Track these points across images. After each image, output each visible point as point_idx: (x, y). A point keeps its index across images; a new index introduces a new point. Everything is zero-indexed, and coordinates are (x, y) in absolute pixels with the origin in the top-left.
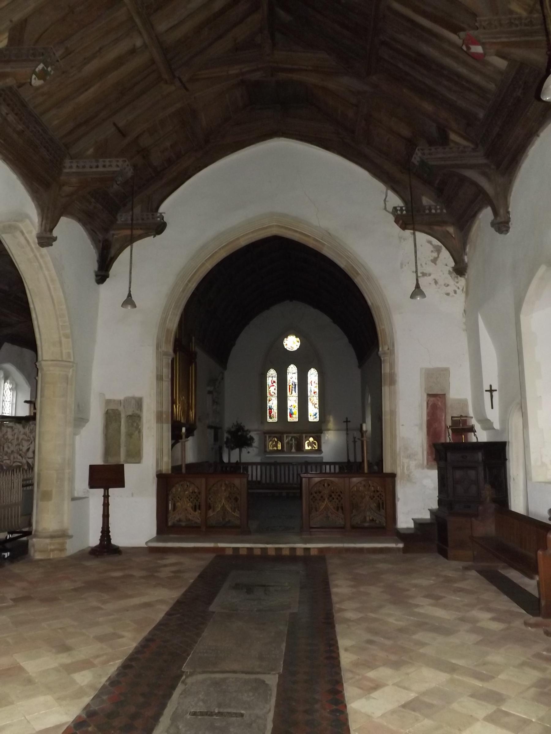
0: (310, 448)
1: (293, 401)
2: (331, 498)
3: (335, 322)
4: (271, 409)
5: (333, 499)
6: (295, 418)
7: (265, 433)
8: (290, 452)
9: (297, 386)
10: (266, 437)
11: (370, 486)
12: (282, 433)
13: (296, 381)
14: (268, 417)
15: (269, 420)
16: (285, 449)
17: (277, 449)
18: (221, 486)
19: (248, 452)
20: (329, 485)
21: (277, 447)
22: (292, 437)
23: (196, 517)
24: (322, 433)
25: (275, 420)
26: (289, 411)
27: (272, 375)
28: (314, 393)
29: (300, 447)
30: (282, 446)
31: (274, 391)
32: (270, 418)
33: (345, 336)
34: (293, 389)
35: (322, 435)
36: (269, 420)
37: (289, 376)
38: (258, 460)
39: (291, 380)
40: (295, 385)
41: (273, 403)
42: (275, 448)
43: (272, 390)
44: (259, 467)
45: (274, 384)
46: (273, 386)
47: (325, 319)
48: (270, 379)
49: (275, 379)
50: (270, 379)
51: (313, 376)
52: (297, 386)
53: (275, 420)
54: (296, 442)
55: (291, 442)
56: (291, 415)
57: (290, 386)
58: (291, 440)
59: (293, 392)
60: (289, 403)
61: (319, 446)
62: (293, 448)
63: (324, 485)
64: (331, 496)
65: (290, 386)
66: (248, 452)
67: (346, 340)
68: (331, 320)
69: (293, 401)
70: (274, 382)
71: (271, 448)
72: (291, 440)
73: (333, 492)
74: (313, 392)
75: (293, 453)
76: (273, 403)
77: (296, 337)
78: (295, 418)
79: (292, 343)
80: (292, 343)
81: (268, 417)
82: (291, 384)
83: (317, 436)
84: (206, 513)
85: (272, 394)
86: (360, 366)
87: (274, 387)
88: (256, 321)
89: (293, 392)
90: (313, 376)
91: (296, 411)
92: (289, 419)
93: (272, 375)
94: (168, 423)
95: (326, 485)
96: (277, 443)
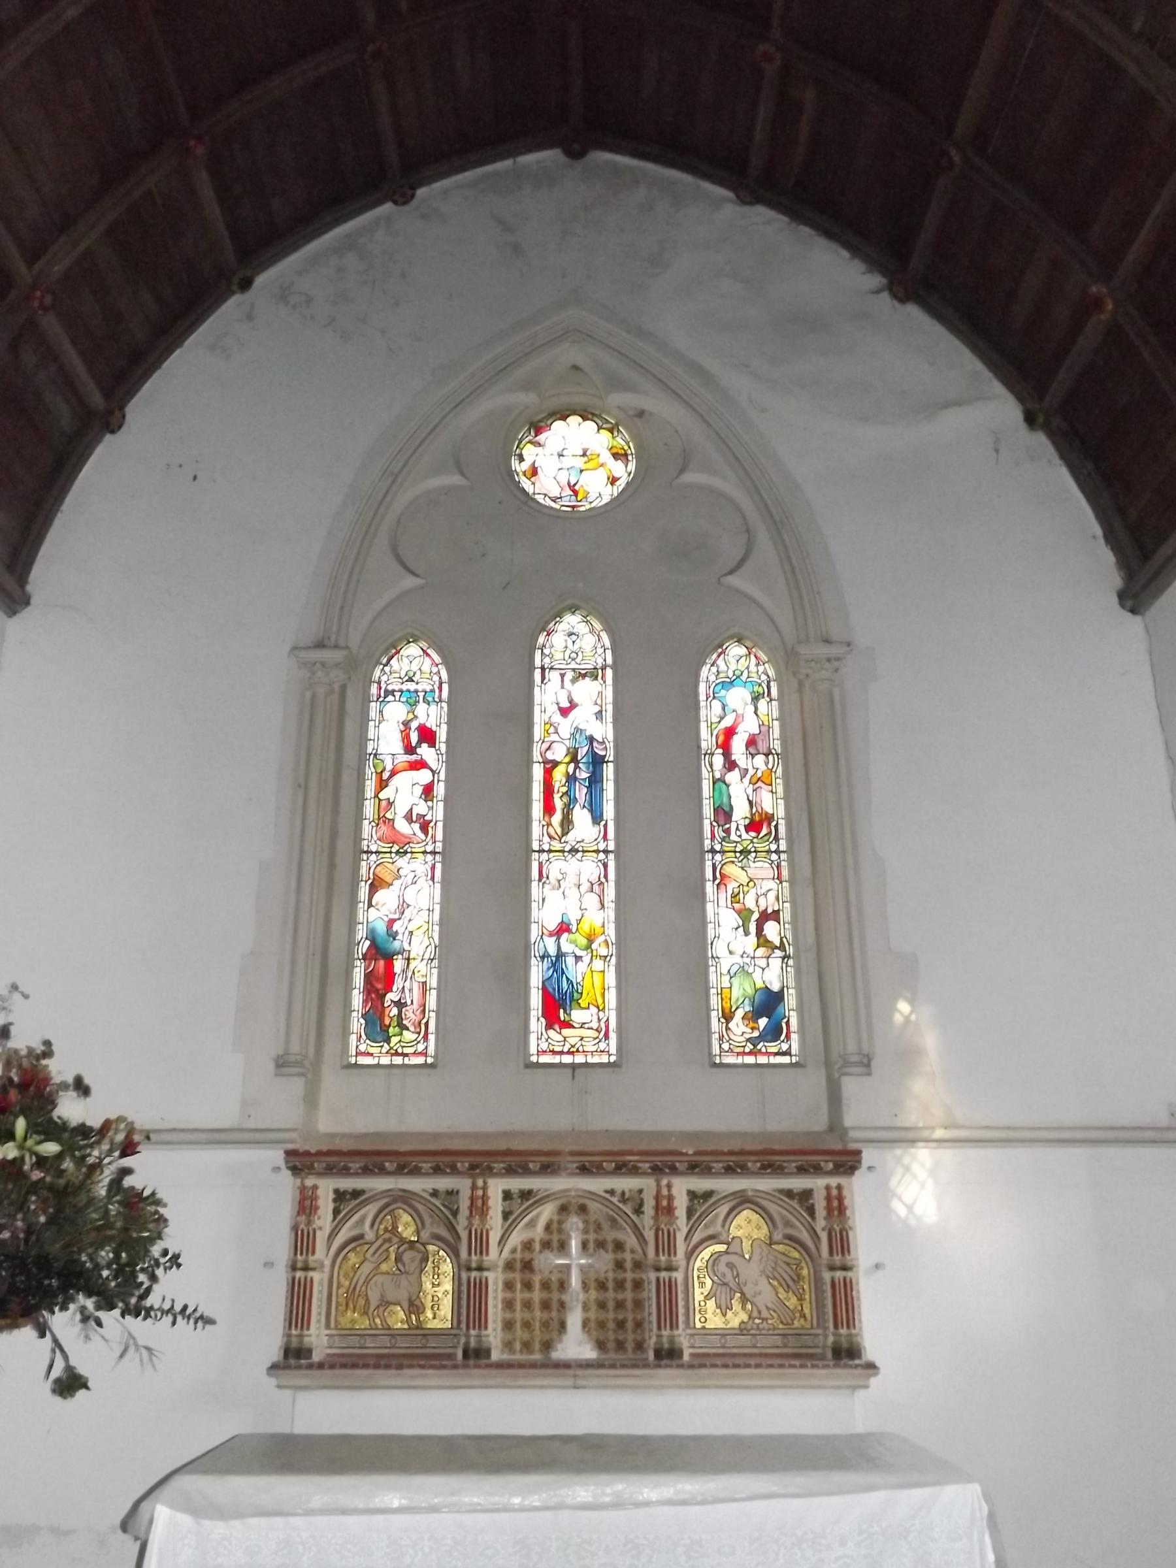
0: (737, 1317)
1: (572, 893)
4: (382, 956)
8: (536, 1360)
12: (480, 1161)
13: (604, 731)
14: (357, 1024)
16: (494, 1336)
17: (419, 1331)
19: (70, 1384)
21: (414, 1306)
22: (564, 1209)
24: (847, 1162)
26: (537, 975)
27: (412, 685)
28: (754, 826)
30: (470, 1299)
31: (422, 808)
32: (377, 1028)
33: (998, 388)
34: (581, 793)
35: (858, 1188)
37: (547, 696)
39: (565, 726)
40: (597, 762)
45: (425, 752)
46: (420, 765)
47: (832, 274)
48: (396, 711)
49: (432, 716)
50: (396, 711)
51: (737, 694)
52: (609, 771)
54: (604, 1262)
56: (556, 1007)
57: (550, 767)
59: (581, 816)
60: (548, 908)
61: (841, 1302)
62: (574, 1320)
65: (550, 767)
66: (70, 1384)
67: (1002, 408)
68: (876, 280)
69: (572, 893)
70: (427, 736)
72: (556, 1242)
74: (741, 812)
79: (574, 462)
80: (574, 462)
82: (559, 753)
85: (402, 826)
86: (1135, 596)
87: (424, 776)
89: (581, 816)
90: (737, 694)
91: (596, 977)
93: (412, 685)
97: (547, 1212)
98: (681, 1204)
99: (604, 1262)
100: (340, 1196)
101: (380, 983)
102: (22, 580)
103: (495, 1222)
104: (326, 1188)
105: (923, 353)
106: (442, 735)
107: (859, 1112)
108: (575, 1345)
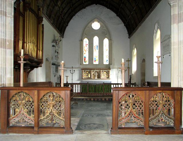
2: (134, 106)
3: (117, 16)
5: (136, 106)
6: (97, 63)
7: (82, 69)
8: (94, 79)
9: (98, 47)
10: (83, 71)
11: (163, 96)
12: (91, 69)
14: (84, 62)
15: (84, 63)
16: (92, 77)
18: (50, 96)
20: (133, 96)
21: (88, 76)
23: (30, 120)
25: (87, 63)
26: (94, 59)
27: (86, 41)
29: (99, 77)
30: (91, 76)
32: (85, 62)
33: (123, 23)
36: (84, 63)
38: (79, 82)
41: (86, 54)
42: (87, 77)
43: (86, 48)
44: (79, 85)
47: (113, 14)
53: (87, 63)
55: (95, 74)
56: (95, 60)
58: (95, 73)
62: (96, 77)
63: (129, 96)
64: (134, 104)
71: (85, 77)
72: (95, 73)
73: (136, 102)
75: (96, 79)
76: (86, 54)
77: (98, 22)
78: (97, 63)
79: (96, 26)
80: (96, 26)
81: (84, 62)
83: (108, 71)
84: (39, 117)
85: (86, 50)
86: (129, 38)
87: (87, 47)
88: (79, 14)
90: (106, 41)
91: (97, 59)
92: (94, 63)
94: (10, 49)
95: (131, 96)
96: (88, 74)
97: (95, 72)
98: (101, 71)
99: (97, 74)
100: (84, 71)
101: (85, 60)
102: (63, 36)
103: (92, 72)
104: (83, 71)
105: (118, 20)
106: (88, 45)
107: (111, 66)
108: (96, 78)
